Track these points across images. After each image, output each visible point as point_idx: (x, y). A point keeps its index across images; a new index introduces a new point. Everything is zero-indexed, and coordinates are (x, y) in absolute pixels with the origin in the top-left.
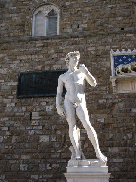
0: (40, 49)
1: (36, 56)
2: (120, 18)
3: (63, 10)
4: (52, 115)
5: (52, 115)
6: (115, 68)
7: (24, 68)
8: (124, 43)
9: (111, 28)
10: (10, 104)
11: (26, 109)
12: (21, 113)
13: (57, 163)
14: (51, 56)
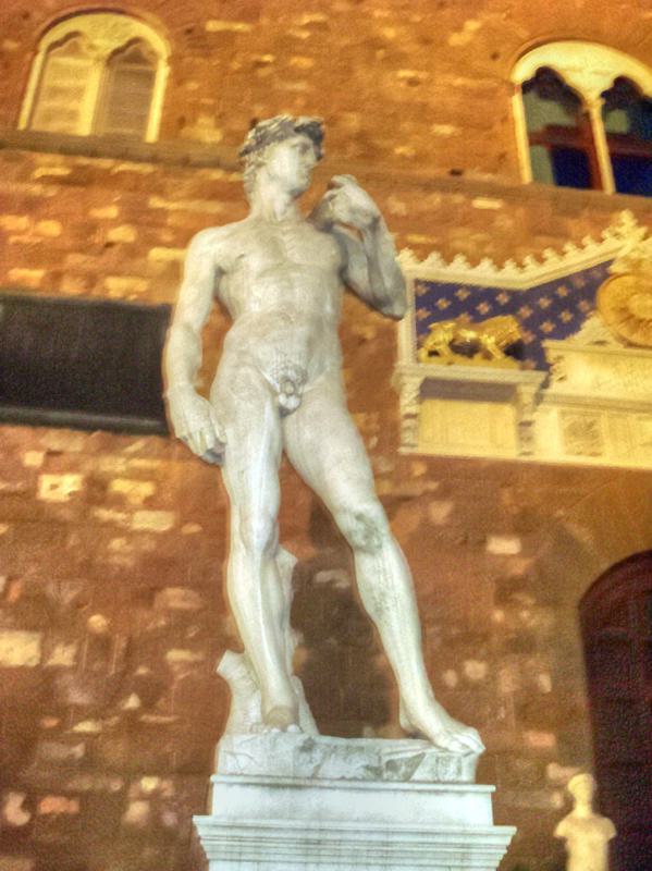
0: (52, 192)
2: (446, 130)
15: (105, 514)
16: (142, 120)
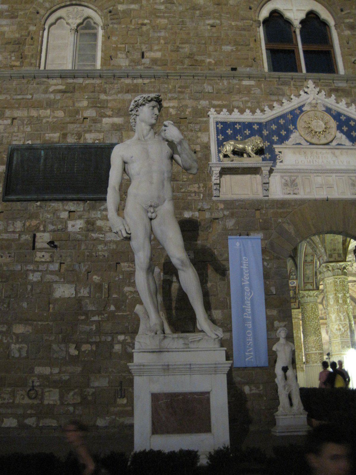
0: (58, 96)
1: (48, 112)
2: (228, 48)
3: (111, 19)
6: (218, 147)
7: (21, 135)
8: (237, 97)
9: (210, 63)
11: (24, 225)
12: (13, 235)
13: (91, 343)
14: (82, 113)
15: (94, 235)
16: (94, 58)
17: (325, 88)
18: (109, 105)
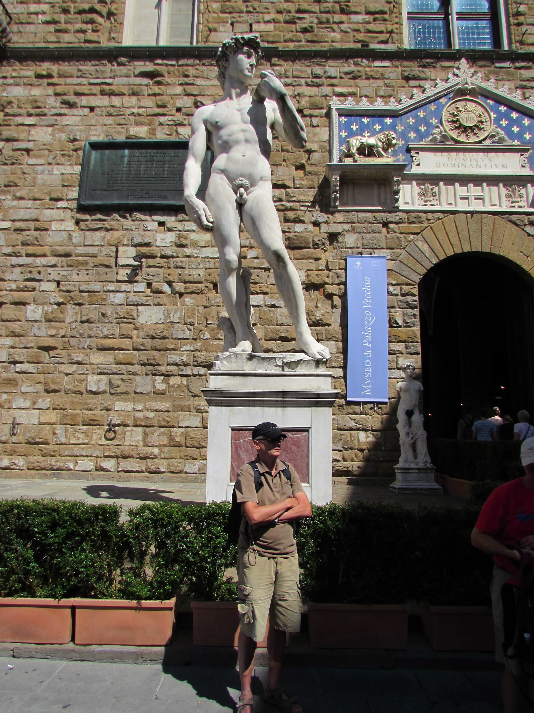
0: (146, 81)
1: (134, 99)
4: (173, 257)
5: (173, 257)
8: (367, 82)
10: (62, 224)
11: (104, 238)
15: (188, 251)
17: (482, 69)
18: (208, 93)
